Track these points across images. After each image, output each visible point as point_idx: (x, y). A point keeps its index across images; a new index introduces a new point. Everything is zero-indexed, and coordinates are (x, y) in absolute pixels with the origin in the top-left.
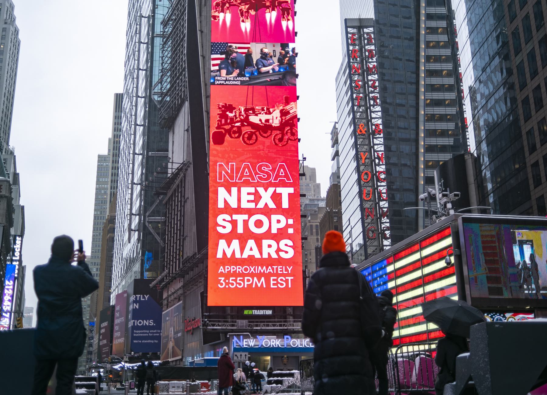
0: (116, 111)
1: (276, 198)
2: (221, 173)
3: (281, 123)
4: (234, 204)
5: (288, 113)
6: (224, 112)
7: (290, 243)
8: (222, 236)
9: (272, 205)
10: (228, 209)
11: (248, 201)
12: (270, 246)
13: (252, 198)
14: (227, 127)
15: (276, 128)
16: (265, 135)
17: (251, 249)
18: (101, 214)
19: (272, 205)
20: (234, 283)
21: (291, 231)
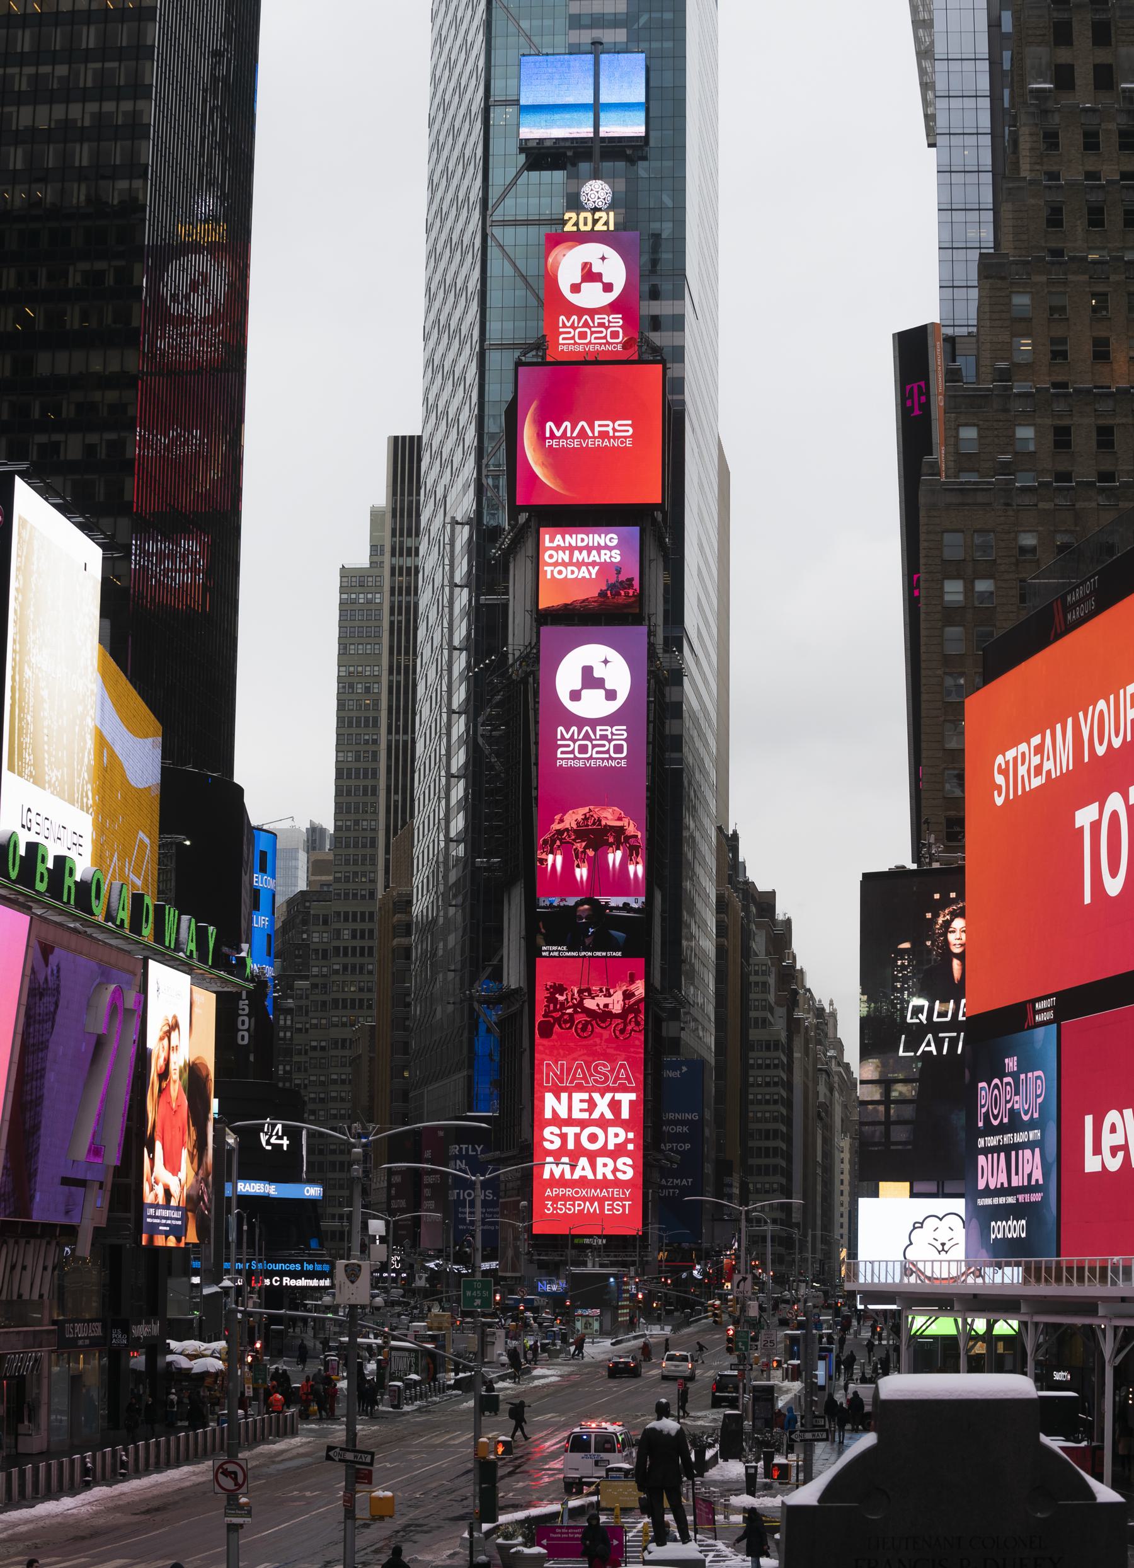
0: (394, 494)
1: (615, 1106)
2: (548, 1075)
3: (623, 1008)
4: (563, 1114)
5: (633, 995)
6: (553, 994)
7: (629, 1161)
8: (550, 1153)
9: (609, 1115)
10: (556, 1121)
11: (581, 1110)
12: (605, 1165)
13: (585, 1106)
14: (557, 1015)
15: (617, 1016)
16: (603, 1025)
17: (583, 1169)
18: (357, 759)
19: (609, 1115)
20: (563, 1208)
21: (631, 1147)
